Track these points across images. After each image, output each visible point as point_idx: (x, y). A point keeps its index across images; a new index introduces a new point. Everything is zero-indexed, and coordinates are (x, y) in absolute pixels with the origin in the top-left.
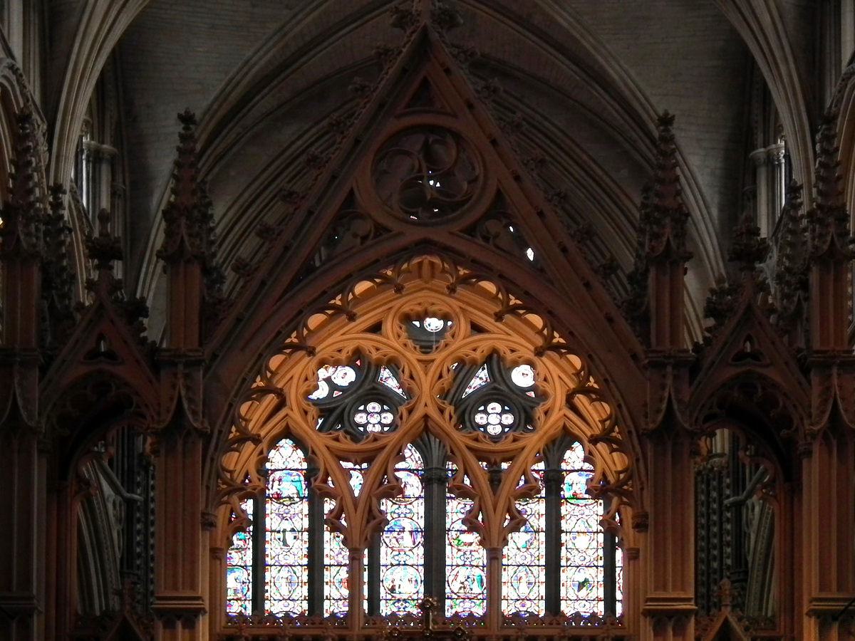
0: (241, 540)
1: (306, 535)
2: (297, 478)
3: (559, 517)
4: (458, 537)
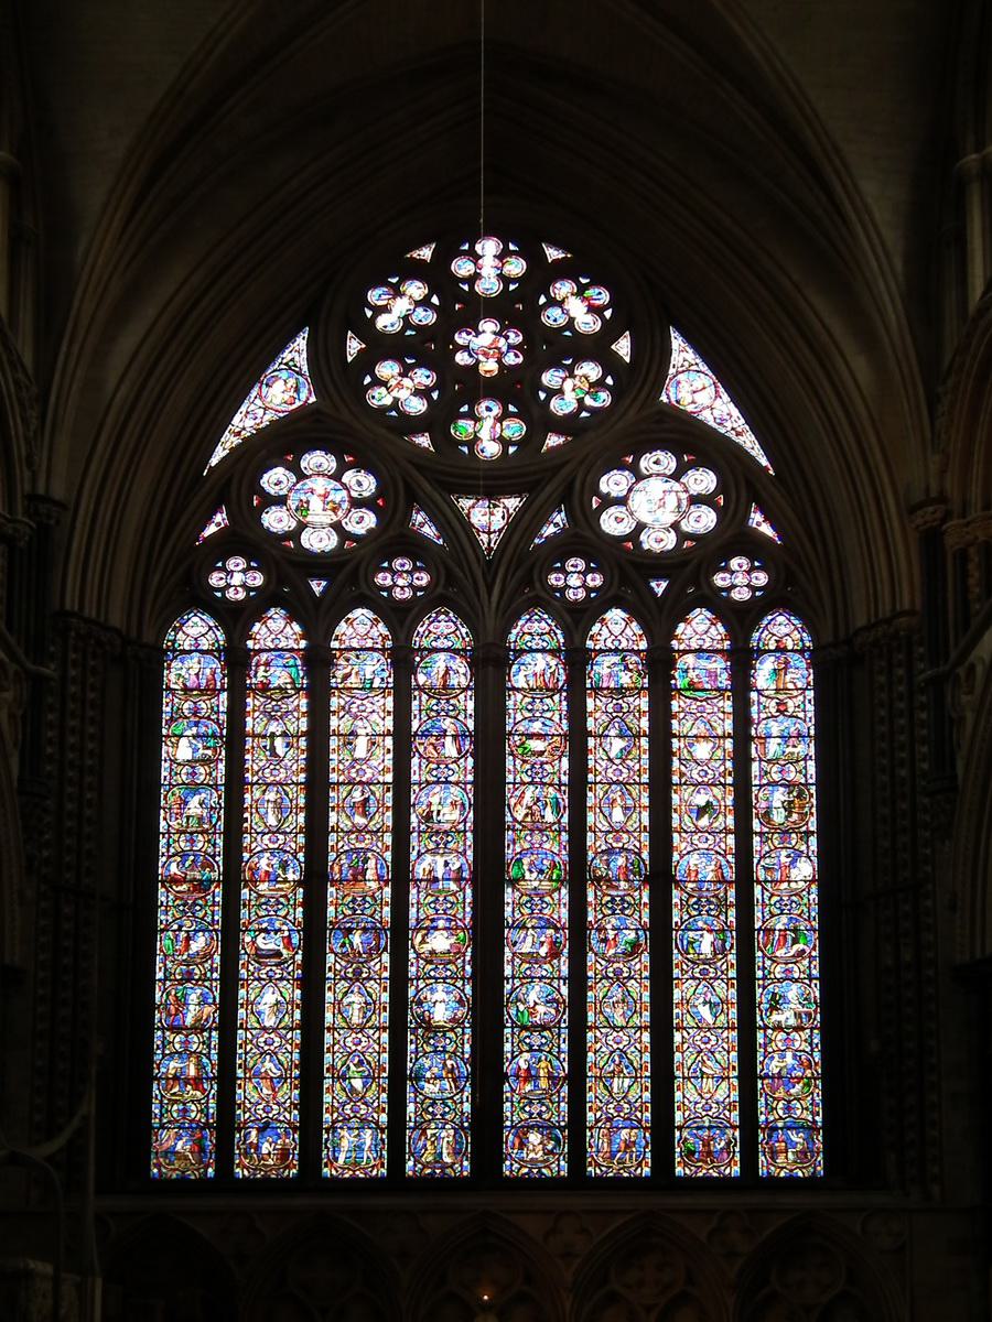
0: (208, 748)
2: (291, 662)
3: (670, 716)
4: (523, 743)
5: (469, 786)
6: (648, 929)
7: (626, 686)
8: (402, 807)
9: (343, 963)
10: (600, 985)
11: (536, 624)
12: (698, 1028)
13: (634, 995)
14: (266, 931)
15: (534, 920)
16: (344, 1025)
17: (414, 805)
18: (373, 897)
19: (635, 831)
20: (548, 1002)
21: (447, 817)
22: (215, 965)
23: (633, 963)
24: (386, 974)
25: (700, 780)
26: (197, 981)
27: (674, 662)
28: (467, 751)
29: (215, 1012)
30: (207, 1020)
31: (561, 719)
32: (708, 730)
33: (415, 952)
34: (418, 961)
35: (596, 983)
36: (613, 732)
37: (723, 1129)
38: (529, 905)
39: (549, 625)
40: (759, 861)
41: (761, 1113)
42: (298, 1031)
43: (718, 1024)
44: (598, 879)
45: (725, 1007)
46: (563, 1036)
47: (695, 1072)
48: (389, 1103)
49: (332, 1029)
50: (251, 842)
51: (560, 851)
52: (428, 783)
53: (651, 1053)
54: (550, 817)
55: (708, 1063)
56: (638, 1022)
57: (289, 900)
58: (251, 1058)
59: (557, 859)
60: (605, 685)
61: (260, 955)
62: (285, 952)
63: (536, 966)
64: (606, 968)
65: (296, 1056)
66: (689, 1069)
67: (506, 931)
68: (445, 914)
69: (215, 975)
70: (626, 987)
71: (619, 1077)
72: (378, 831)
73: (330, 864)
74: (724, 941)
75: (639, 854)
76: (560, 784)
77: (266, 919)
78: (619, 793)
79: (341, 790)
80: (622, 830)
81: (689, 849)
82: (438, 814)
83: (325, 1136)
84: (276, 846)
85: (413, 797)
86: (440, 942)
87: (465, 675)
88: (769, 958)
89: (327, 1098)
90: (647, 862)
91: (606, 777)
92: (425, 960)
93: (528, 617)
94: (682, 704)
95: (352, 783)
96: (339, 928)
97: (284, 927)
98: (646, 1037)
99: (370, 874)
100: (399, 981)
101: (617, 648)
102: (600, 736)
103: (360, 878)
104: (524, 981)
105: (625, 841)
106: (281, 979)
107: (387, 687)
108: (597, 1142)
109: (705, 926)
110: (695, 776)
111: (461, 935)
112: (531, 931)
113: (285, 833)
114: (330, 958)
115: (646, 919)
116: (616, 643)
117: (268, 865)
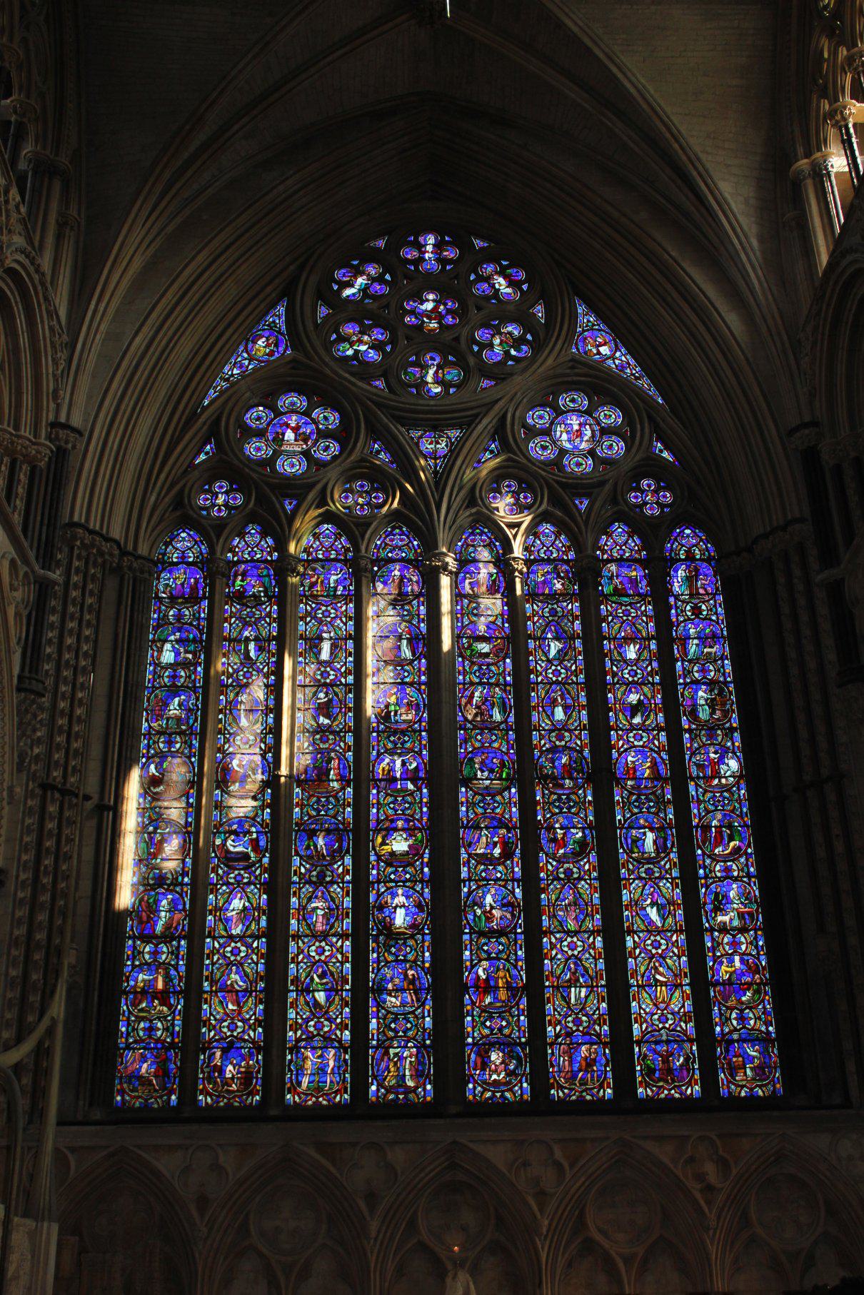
4: (470, 645)
11: (478, 537)
12: (648, 931)
13: (585, 897)
14: (235, 833)
15: (487, 820)
16: (308, 932)
18: (336, 797)
19: (575, 729)
20: (503, 905)
21: (404, 717)
24: (348, 878)
25: (630, 679)
26: (169, 885)
29: (185, 919)
31: (503, 623)
33: (376, 854)
34: (378, 864)
35: (548, 885)
36: (549, 636)
41: (716, 1025)
42: (264, 940)
44: (546, 777)
46: (519, 942)
47: (649, 979)
49: (296, 937)
50: (225, 743)
51: (508, 749)
54: (497, 716)
55: (661, 969)
58: (218, 969)
59: (506, 758)
61: (230, 860)
62: (252, 855)
63: (491, 868)
64: (557, 868)
66: (643, 977)
67: (461, 831)
68: (403, 814)
70: (577, 888)
71: (576, 987)
72: (341, 731)
74: (665, 839)
75: (581, 752)
76: (506, 684)
80: (563, 729)
83: (289, 1057)
87: (417, 582)
88: (709, 857)
89: (291, 1014)
91: (547, 677)
96: (304, 830)
97: (254, 829)
100: (361, 885)
101: (549, 558)
102: (539, 639)
103: (324, 778)
105: (567, 739)
106: (249, 884)
108: (559, 1059)
111: (419, 835)
112: (485, 832)
114: (296, 860)
116: (548, 553)
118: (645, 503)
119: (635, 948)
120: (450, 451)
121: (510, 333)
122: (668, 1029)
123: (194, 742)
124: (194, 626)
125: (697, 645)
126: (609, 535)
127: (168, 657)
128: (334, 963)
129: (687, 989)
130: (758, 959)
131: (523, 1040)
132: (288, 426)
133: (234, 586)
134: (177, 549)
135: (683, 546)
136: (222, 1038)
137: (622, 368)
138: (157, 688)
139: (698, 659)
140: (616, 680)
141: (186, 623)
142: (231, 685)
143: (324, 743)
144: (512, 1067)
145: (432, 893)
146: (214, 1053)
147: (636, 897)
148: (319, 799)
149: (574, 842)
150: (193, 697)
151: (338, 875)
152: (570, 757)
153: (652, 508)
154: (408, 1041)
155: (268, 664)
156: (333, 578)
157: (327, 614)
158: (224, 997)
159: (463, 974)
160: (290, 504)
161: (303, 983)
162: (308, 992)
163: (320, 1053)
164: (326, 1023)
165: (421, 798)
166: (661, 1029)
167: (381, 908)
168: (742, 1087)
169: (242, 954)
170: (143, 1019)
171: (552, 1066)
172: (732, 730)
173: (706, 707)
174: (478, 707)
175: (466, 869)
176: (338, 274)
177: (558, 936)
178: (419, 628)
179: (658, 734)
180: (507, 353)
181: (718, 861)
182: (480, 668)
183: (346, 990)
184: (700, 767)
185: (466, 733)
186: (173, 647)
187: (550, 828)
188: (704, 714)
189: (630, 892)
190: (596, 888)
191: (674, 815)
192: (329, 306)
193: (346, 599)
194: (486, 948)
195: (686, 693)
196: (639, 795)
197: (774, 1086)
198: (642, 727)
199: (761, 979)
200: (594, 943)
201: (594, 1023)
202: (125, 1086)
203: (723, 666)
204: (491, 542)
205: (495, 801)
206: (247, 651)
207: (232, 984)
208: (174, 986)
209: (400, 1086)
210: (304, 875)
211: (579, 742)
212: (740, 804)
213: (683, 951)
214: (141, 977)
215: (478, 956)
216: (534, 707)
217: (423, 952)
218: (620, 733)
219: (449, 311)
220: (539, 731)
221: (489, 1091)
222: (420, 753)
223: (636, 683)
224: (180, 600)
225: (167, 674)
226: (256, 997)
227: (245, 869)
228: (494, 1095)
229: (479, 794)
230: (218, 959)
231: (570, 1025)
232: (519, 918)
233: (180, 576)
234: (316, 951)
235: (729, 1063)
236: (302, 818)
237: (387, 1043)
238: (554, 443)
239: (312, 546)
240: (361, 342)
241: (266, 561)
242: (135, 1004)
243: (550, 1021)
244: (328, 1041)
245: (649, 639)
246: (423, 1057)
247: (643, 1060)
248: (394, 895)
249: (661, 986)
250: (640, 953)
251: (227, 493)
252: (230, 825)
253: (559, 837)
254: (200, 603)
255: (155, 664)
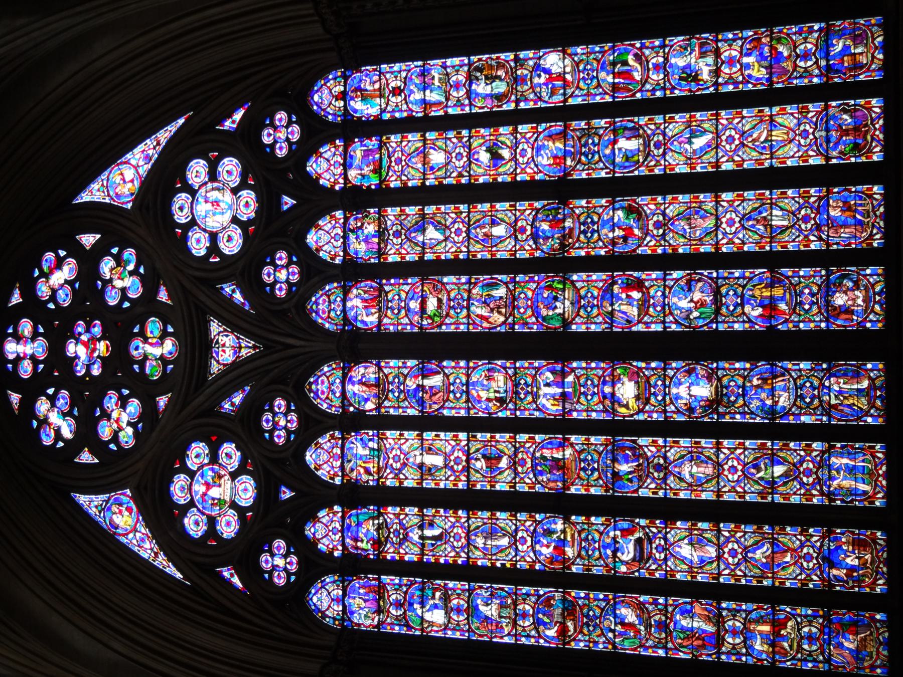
1: (429, 512)
3: (405, 188)
4: (430, 317)
5: (471, 364)
6: (613, 199)
7: (377, 228)
8: (492, 425)
9: (649, 481)
10: (671, 242)
11: (320, 307)
12: (717, 147)
13: (682, 209)
15: (605, 303)
17: (490, 414)
19: (515, 215)
20: (690, 290)
21: (501, 384)
22: (651, 600)
23: (648, 212)
24: (661, 441)
25: (465, 159)
26: (667, 618)
27: (354, 186)
28: (437, 366)
29: (700, 603)
30: (710, 612)
31: (408, 284)
32: (418, 154)
33: (637, 413)
34: (647, 412)
35: (670, 245)
37: (828, 118)
38: (589, 309)
39: (322, 296)
40: (546, 102)
42: (722, 525)
43: (713, 129)
44: (563, 246)
45: (694, 123)
46: (726, 275)
47: (764, 148)
48: (801, 440)
49: (719, 493)
50: (525, 561)
51: (534, 282)
52: (468, 401)
53: (744, 190)
54: (501, 292)
55: (755, 136)
56: (711, 205)
57: (584, 529)
58: (750, 571)
59: (543, 284)
60: (376, 246)
61: (641, 558)
62: (637, 535)
63: (652, 301)
64: (653, 236)
65: (749, 529)
67: (615, 330)
68: (598, 386)
69: (661, 601)
70: (673, 217)
71: (771, 220)
72: (514, 446)
73: (547, 490)
74: (626, 128)
75: (538, 210)
76: (469, 282)
77: (602, 550)
78: (478, 230)
79: (474, 479)
81: (532, 165)
82: (498, 392)
83: (838, 503)
84: (529, 539)
85: (481, 414)
86: (627, 390)
87: (366, 368)
88: (643, 85)
89: (795, 499)
90: (546, 202)
91: (462, 242)
92: (646, 404)
93: (314, 314)
94: (393, 178)
95: (467, 469)
97: (612, 534)
98: (727, 196)
99: (559, 455)
102: (423, 249)
104: (667, 312)
106: (666, 539)
107: (378, 436)
108: (842, 239)
109: (610, 147)
110: (462, 163)
111: (619, 371)
112: (616, 307)
113: (516, 531)
114: (643, 492)
115: (603, 201)
116: (337, 238)
117: (548, 547)
118: (287, 140)
119: (734, 161)
120: (232, 333)
121: (112, 270)
122: (815, 129)
123: (524, 591)
124: (407, 590)
125: (431, 91)
126: (320, 176)
127: (438, 617)
128: (745, 457)
129: (776, 109)
130: (746, 39)
131: (823, 272)
132: (205, 494)
133: (367, 550)
134: (329, 606)
135: (331, 103)
136: (819, 567)
137: (148, 158)
138: (470, 627)
139: (445, 92)
140: (466, 174)
141: (405, 598)
142: (467, 554)
143: (526, 463)
144: (850, 284)
145: (676, 359)
146: (834, 576)
147: (683, 158)
148: (581, 469)
149: (627, 218)
150: (479, 591)
151: (658, 451)
152: (543, 221)
153: (292, 133)
154: (823, 385)
155: (446, 517)
156: (362, 451)
157: (396, 458)
158: (779, 565)
159: (757, 331)
160: (284, 493)
161: (765, 488)
162: (774, 482)
163: (834, 473)
164: (805, 465)
165: (582, 368)
166: (815, 137)
167: (691, 410)
168: (873, 57)
169: (736, 547)
170: (799, 646)
171: (849, 244)
172: (517, 59)
173: (494, 84)
174: (492, 310)
175: (653, 326)
176: (47, 441)
177: (720, 236)
178: (412, 368)
179: (521, 133)
180: (131, 273)
181: (648, 77)
182: (453, 307)
183: (772, 445)
184: (553, 93)
185: (518, 323)
186: (428, 611)
187: (613, 242)
188: (500, 87)
189: (678, 164)
190: (673, 199)
191: (602, 119)
192: (79, 451)
193: (382, 439)
194: (732, 308)
195: (479, 105)
196: (581, 154)
197: (873, 25)
198: (514, 147)
199: (766, 36)
200: (728, 201)
201: (807, 202)
202: (866, 664)
203: (453, 67)
204: (325, 294)
205: (586, 296)
206: (434, 538)
207: (766, 558)
208: (767, 614)
209: (868, 394)
210: (657, 484)
211: (528, 212)
212: (591, 53)
213: (737, 113)
214: (758, 647)
215: (740, 315)
216: (492, 255)
217: (735, 369)
218: (518, 171)
219: (88, 330)
220: (516, 251)
221: (873, 307)
222: (539, 368)
223: (469, 153)
224: (382, 603)
225: (455, 617)
226: (779, 534)
227: (650, 542)
228: (879, 302)
229: (579, 311)
230: (740, 570)
231: (809, 226)
232: (702, 274)
233: (355, 603)
234: (733, 474)
235: (850, 70)
236: (601, 486)
237: (825, 406)
238: (224, 228)
239: (328, 472)
240: (118, 421)
241: (343, 518)
242: (786, 653)
243: (805, 246)
244: (822, 463)
245: (425, 140)
246: (839, 371)
247: (845, 155)
248: (678, 397)
249: (771, 136)
250: (738, 156)
251: (273, 555)
252: (608, 557)
253: (622, 233)
254: (385, 584)
255: (445, 629)
